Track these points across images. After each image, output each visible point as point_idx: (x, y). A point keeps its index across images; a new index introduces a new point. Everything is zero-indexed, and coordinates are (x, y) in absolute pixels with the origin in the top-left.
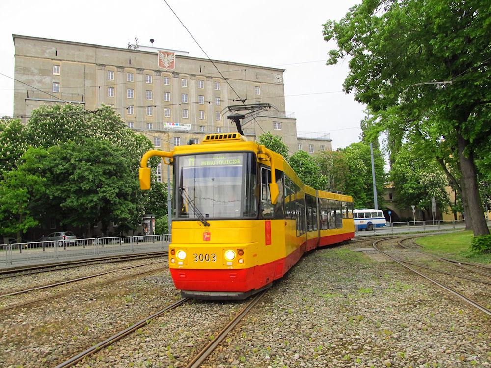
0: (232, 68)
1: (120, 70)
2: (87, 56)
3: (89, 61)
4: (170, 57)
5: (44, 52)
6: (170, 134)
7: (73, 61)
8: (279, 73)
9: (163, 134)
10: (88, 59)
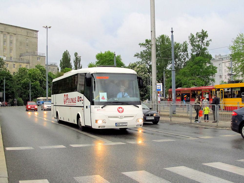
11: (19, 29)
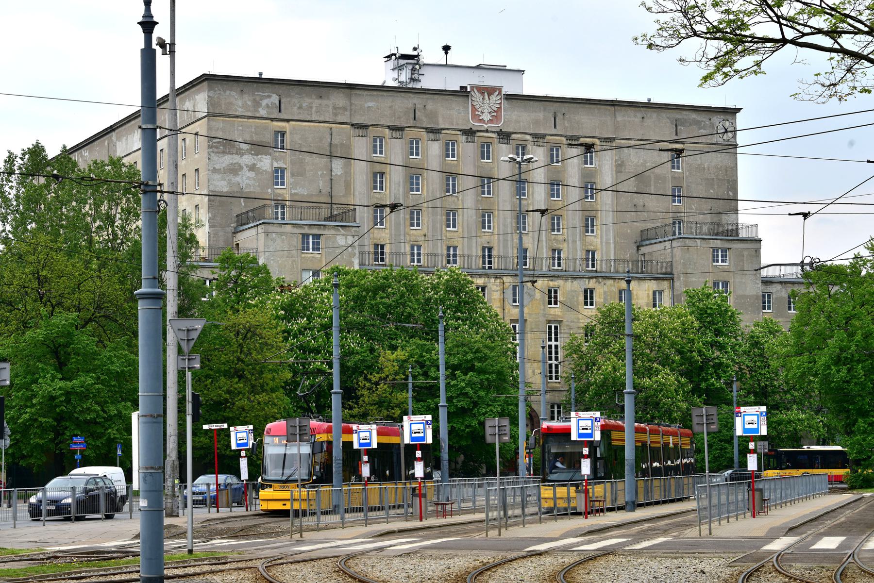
0: (622, 116)
1: (396, 134)
2: (335, 108)
3: (339, 119)
4: (494, 97)
5: (257, 104)
6: (505, 278)
7: (309, 121)
8: (729, 117)
9: (492, 280)
10: (336, 115)
11: (631, 111)
